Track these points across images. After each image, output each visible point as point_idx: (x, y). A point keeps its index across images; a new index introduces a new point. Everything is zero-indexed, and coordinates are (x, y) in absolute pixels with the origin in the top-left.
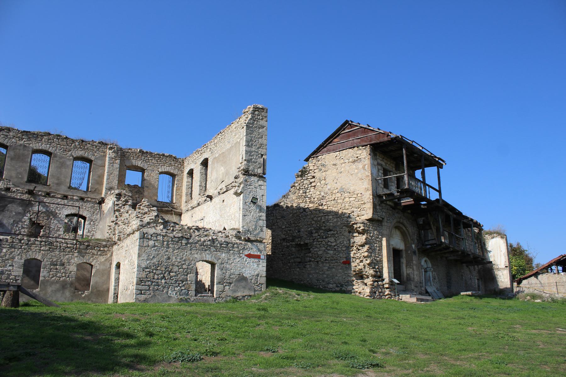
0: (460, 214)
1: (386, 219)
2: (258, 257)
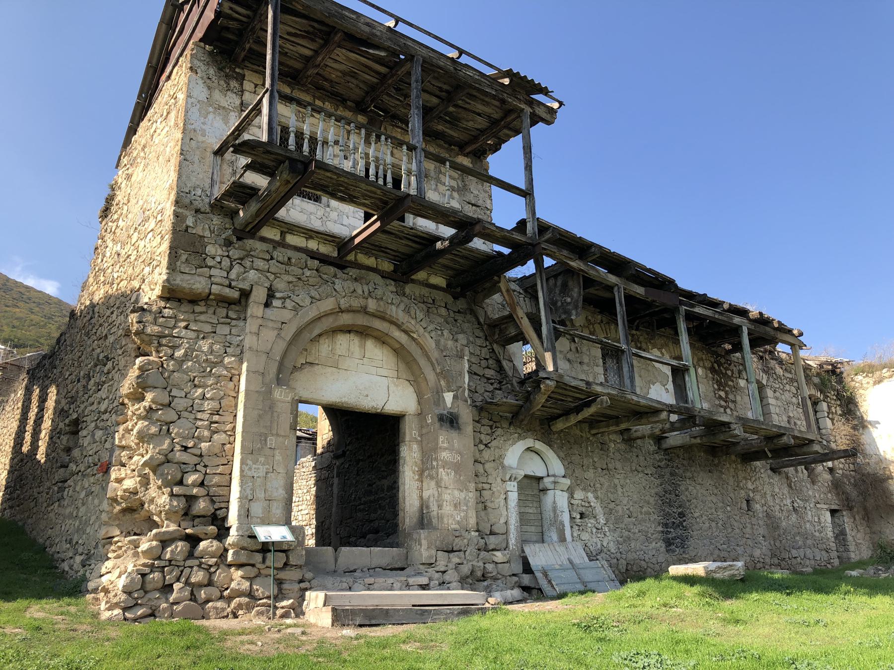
0: (664, 284)
1: (259, 294)
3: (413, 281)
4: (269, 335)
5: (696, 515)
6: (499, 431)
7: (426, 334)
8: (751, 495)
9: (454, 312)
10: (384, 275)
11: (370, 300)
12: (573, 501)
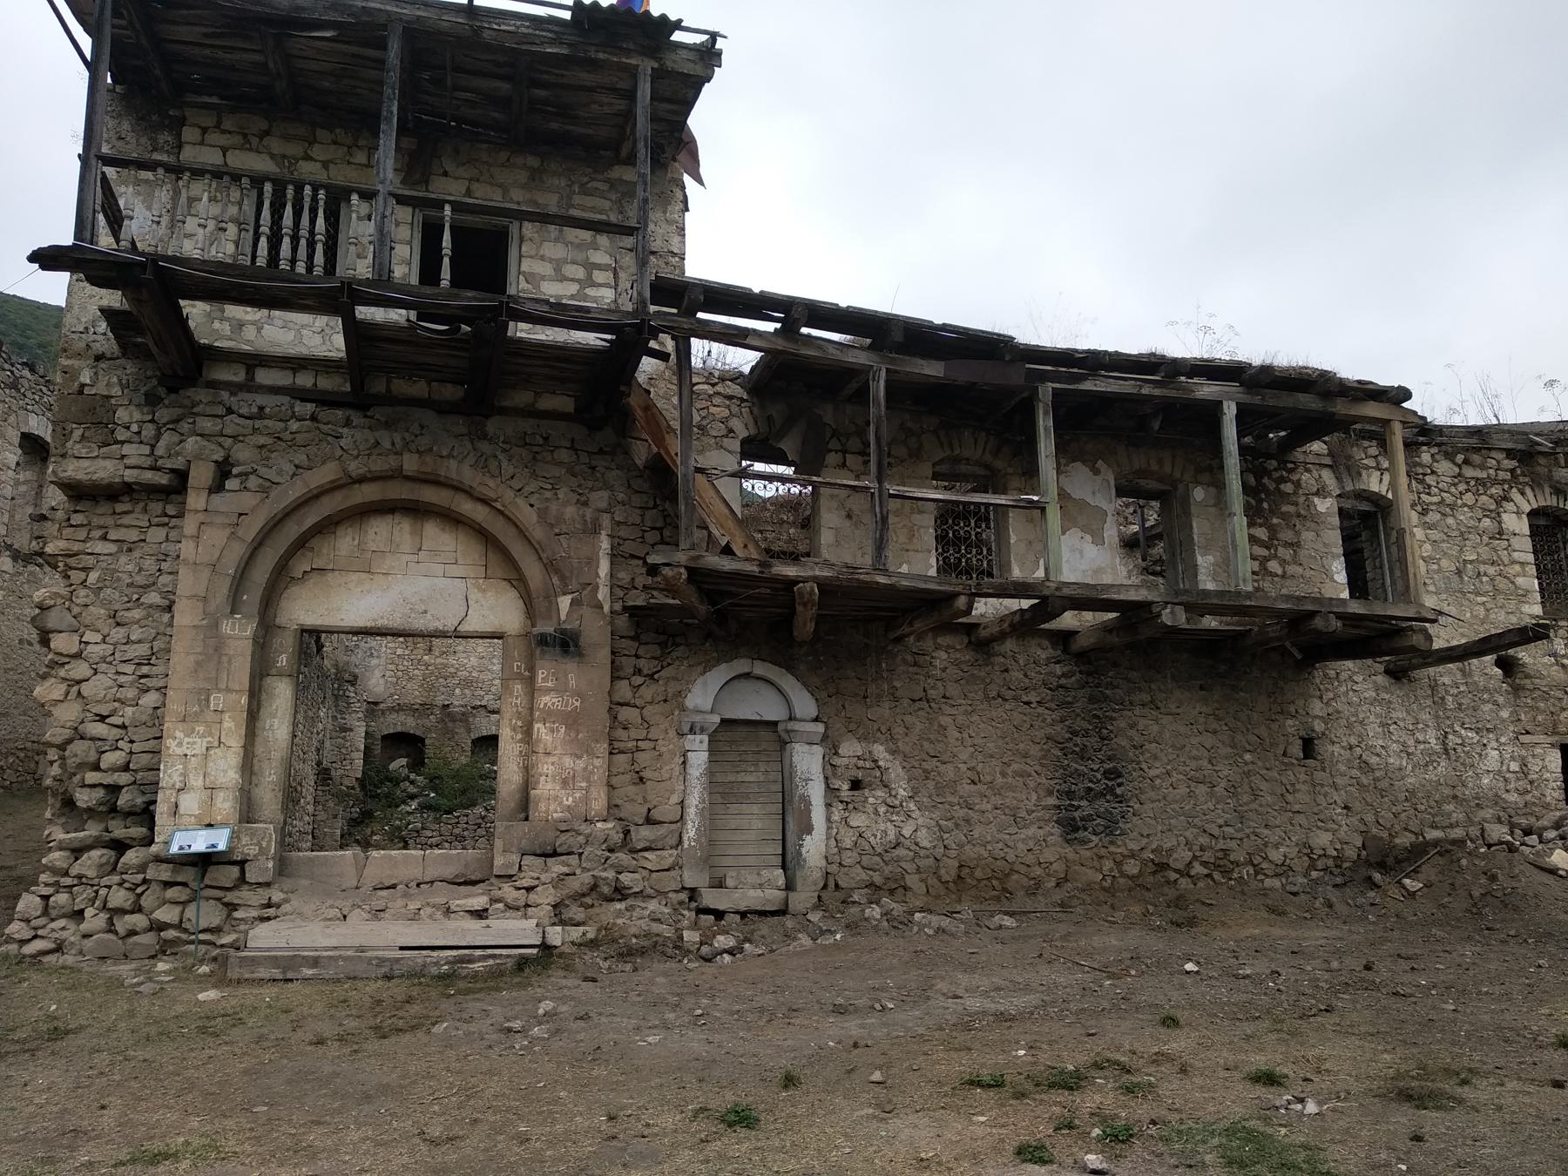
1: (201, 475)
3: (503, 411)
4: (216, 537)
5: (1152, 773)
6: (680, 651)
7: (520, 501)
8: (1319, 726)
9: (590, 453)
10: (443, 409)
11: (406, 456)
12: (836, 761)
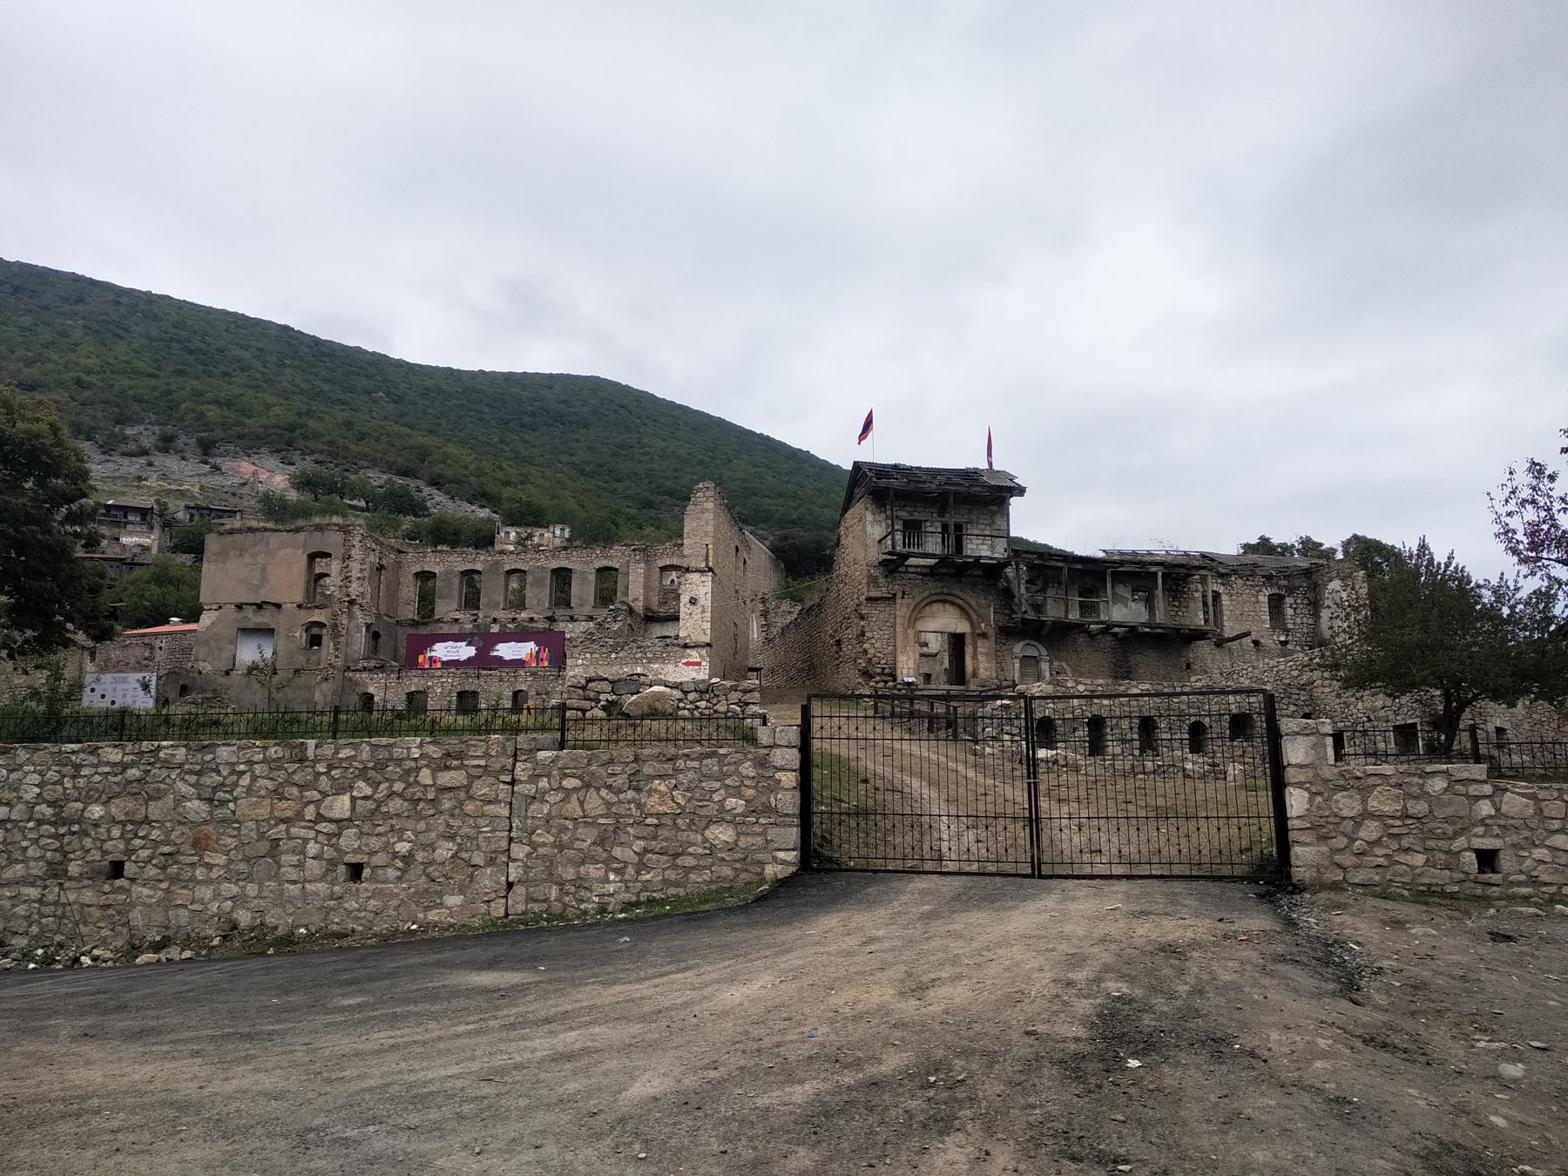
1: (899, 595)
2: (699, 664)
